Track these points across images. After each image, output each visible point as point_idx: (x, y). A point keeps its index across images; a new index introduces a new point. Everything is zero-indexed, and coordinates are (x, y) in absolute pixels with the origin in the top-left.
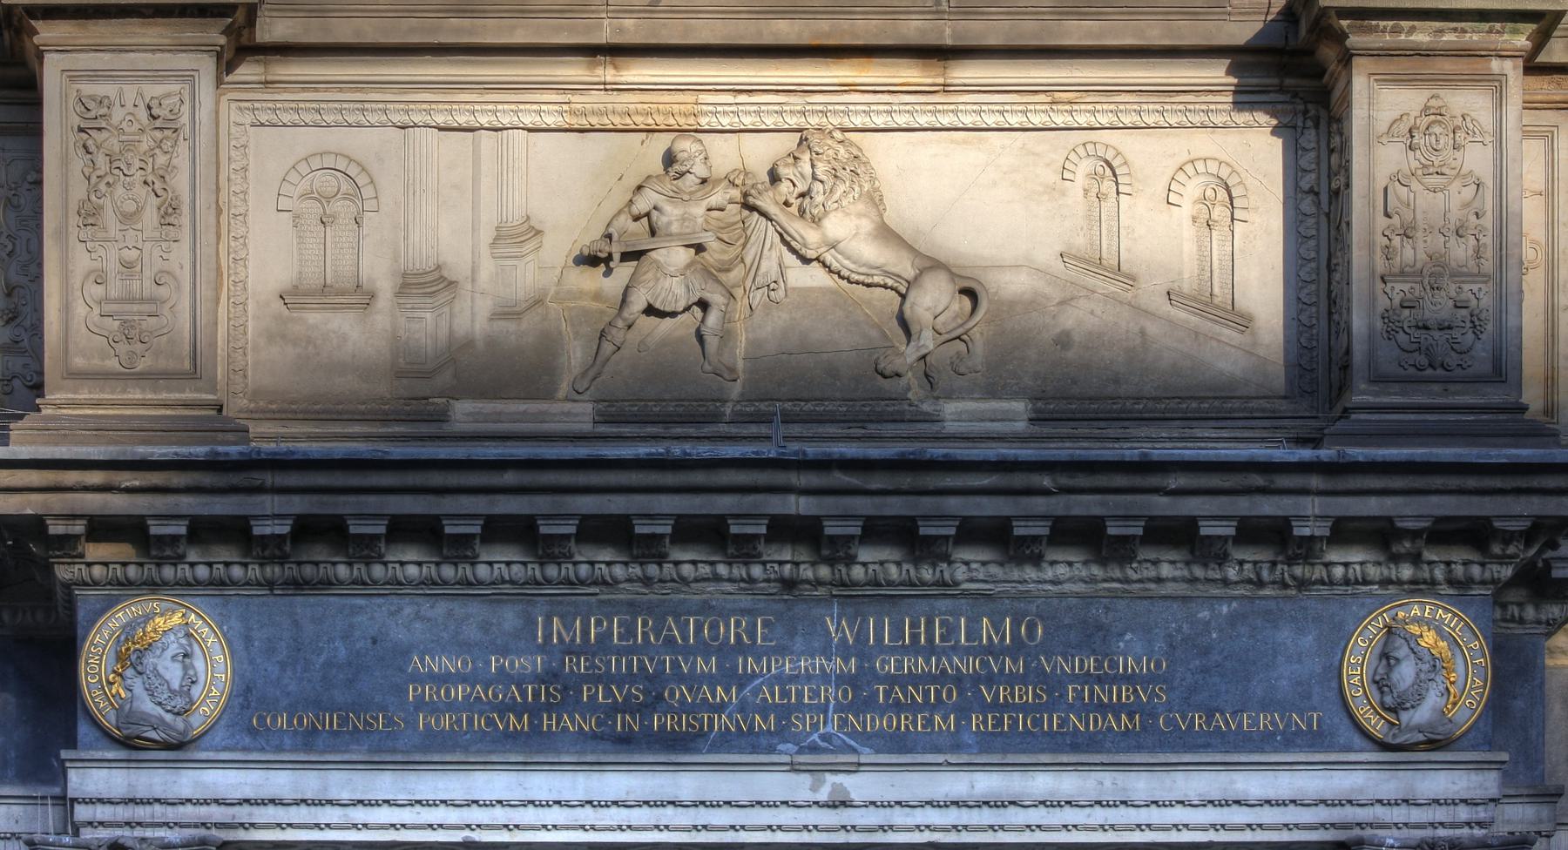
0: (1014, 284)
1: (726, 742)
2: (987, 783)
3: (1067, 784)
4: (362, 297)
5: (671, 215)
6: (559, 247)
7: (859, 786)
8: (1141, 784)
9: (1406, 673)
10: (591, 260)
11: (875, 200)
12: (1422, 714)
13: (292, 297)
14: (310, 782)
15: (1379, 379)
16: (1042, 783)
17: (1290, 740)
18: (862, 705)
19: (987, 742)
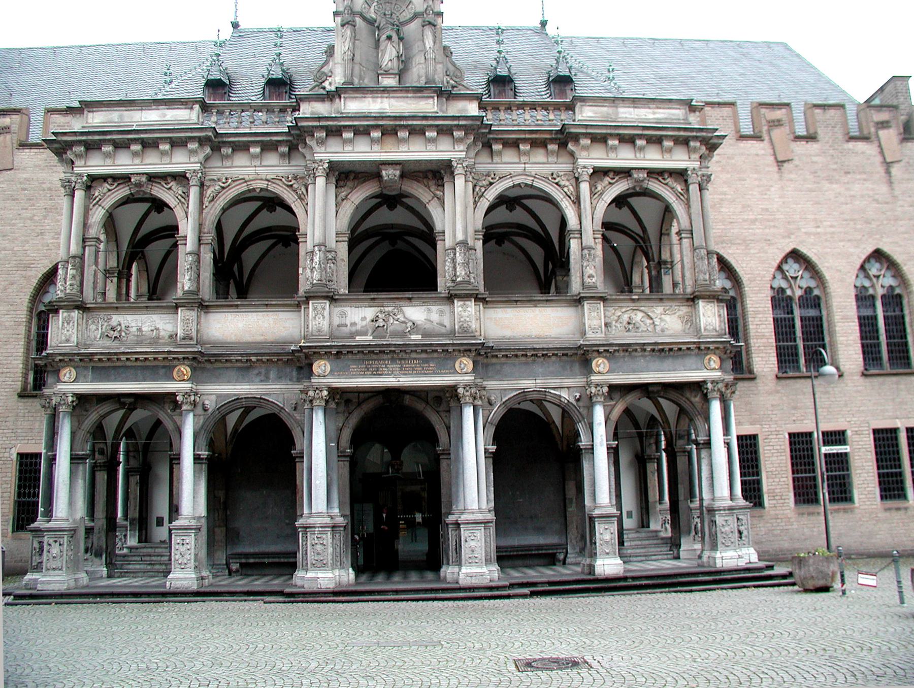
0: (419, 323)
1: (386, 375)
2: (415, 379)
3: (424, 379)
4: (346, 326)
5: (380, 316)
6: (368, 319)
7: (401, 380)
8: (433, 379)
9: (462, 366)
10: (373, 321)
11: (403, 314)
12: (465, 370)
13: (339, 326)
14: (339, 380)
15: (459, 333)
16: (421, 379)
17: (450, 373)
18: (401, 370)
19: (415, 374)
